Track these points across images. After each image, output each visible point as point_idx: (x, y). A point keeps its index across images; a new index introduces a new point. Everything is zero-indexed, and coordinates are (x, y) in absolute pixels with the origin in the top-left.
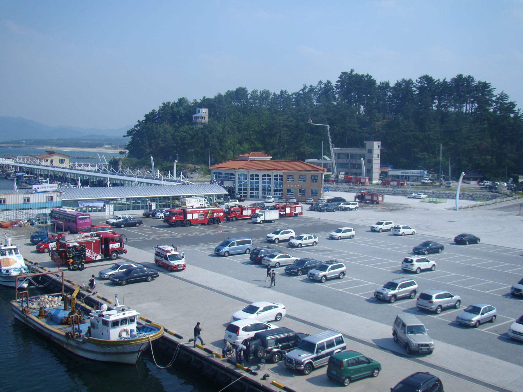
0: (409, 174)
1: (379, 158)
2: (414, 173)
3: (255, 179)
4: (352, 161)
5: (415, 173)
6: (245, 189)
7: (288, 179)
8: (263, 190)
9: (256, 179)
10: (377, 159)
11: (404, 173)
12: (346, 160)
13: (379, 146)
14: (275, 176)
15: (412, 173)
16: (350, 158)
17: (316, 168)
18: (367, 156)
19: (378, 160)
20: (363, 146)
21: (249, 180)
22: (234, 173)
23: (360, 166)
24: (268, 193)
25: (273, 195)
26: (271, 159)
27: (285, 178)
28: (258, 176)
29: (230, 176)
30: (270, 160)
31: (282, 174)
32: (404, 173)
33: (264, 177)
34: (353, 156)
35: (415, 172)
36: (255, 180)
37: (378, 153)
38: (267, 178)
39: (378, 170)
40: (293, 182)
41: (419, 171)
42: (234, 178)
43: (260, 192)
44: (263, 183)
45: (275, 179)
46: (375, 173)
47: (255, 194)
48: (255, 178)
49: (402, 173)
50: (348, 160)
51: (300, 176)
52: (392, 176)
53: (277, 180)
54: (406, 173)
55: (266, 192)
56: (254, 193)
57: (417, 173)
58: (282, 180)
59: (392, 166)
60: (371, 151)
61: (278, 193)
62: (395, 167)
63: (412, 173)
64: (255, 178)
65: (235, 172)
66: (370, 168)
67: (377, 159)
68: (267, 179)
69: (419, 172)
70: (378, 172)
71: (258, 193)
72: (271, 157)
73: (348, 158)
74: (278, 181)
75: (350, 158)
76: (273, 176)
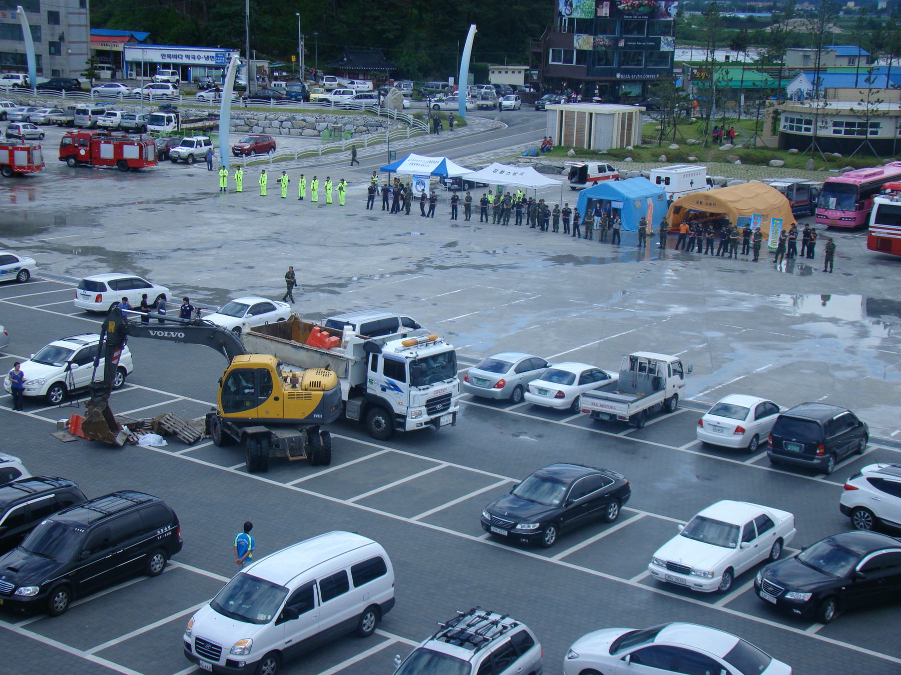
0: (185, 61)
1: (87, 10)
2: (199, 57)
10: (80, 14)
11: (169, 56)
19: (84, 16)
23: (15, 32)
32: (169, 56)
35: (202, 54)
39: (86, 44)
41: (212, 52)
46: (70, 54)
49: (163, 56)
52: (138, 64)
54: (175, 57)
57: (207, 58)
59: (142, 36)
62: (155, 40)
63: (194, 58)
66: (56, 40)
67: (80, 14)
69: (213, 54)
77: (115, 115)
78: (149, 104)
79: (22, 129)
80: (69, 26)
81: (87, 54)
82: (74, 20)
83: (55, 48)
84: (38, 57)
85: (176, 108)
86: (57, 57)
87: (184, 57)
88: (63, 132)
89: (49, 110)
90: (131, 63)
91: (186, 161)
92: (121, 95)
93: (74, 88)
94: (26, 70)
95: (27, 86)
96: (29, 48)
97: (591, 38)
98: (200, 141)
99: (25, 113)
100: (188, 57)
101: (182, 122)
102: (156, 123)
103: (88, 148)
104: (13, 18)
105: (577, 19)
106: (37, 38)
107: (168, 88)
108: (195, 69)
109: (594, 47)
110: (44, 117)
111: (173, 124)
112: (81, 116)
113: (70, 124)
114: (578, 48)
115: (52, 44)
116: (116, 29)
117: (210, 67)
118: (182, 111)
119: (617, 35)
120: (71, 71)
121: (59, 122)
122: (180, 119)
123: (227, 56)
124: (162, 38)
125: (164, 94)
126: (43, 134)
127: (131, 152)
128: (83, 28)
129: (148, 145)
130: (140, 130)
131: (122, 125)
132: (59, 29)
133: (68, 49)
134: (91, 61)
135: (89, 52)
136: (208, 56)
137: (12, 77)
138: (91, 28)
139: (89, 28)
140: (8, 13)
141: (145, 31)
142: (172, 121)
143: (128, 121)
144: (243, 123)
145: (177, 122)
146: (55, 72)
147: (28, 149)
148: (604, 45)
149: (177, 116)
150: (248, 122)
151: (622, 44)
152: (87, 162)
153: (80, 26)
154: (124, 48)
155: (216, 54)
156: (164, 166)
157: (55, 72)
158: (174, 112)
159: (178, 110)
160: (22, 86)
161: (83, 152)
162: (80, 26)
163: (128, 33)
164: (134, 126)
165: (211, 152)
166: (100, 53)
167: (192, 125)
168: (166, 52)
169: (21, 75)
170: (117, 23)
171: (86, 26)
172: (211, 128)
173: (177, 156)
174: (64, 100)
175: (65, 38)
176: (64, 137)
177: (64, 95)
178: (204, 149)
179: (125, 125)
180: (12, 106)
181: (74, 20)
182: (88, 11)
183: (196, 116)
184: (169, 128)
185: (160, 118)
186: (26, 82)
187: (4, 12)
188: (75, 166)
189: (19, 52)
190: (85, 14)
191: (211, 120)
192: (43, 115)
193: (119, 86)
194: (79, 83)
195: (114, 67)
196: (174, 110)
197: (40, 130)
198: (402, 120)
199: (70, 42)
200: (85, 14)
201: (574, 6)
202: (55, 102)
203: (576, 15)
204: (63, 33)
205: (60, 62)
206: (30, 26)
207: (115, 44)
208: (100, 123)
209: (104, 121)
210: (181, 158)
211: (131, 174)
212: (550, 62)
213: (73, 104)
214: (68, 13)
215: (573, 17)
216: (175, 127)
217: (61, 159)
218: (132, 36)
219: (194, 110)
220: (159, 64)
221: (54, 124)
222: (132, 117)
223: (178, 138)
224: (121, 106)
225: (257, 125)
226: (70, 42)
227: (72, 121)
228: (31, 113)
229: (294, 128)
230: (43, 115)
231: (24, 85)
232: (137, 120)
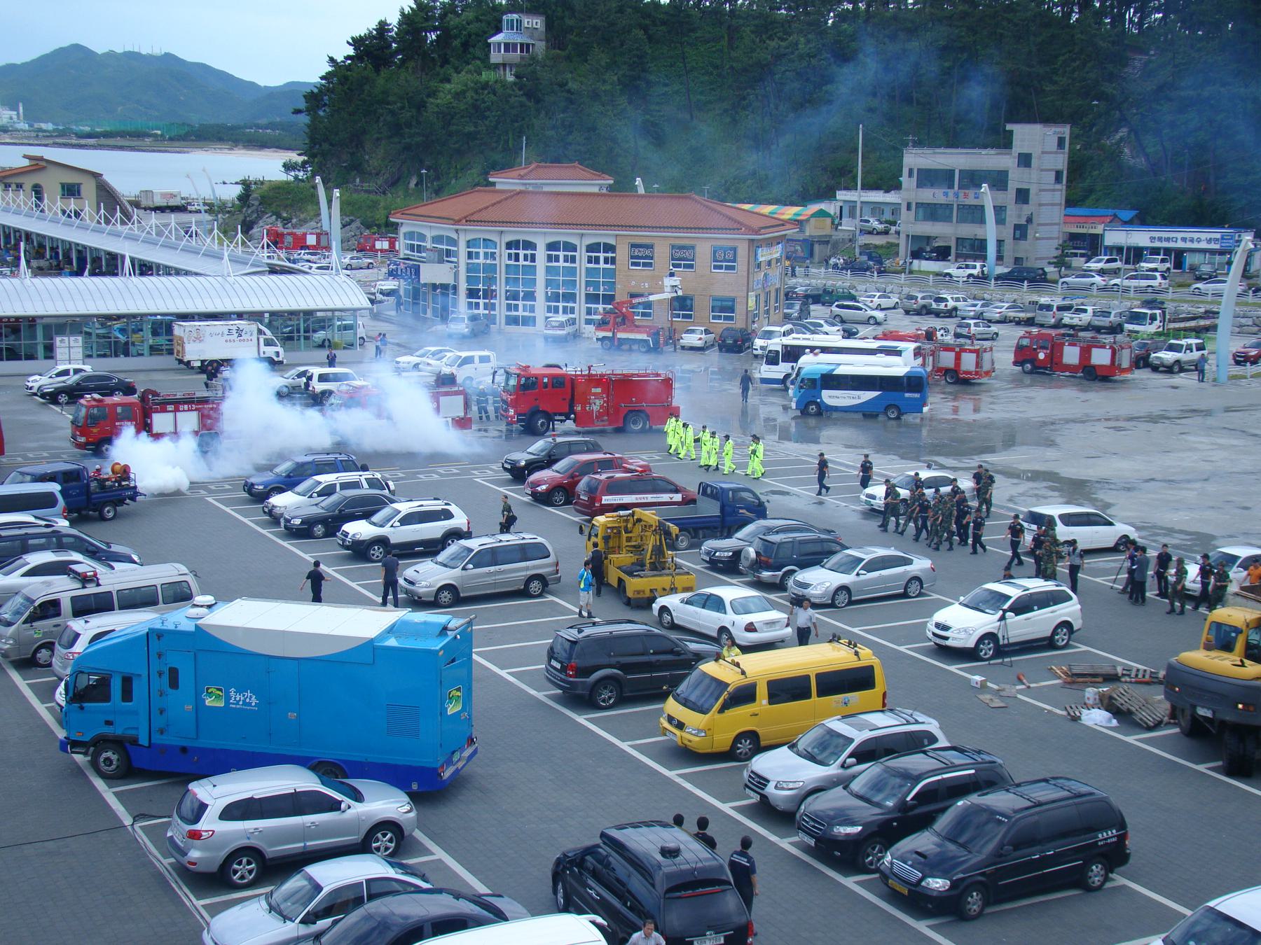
0: (1180, 245)
1: (1062, 187)
2: (1199, 240)
3: (521, 257)
4: (966, 196)
5: (1202, 238)
6: (489, 294)
7: (632, 257)
8: (548, 299)
9: (526, 259)
10: (1054, 190)
11: (1160, 239)
12: (946, 194)
13: (1061, 142)
14: (591, 248)
15: (1192, 240)
17: (730, 218)
20: (1005, 142)
21: (503, 258)
22: (454, 236)
23: (975, 214)
24: (565, 310)
25: (584, 316)
26: (610, 188)
27: (622, 254)
28: (529, 245)
29: (445, 247)
30: (604, 191)
31: (612, 241)
32: (1160, 239)
33: (554, 253)
34: (973, 179)
35: (1203, 236)
36: (522, 262)
37: (1060, 167)
38: (561, 254)
39: (1057, 227)
40: (647, 271)
41: (1216, 233)
42: (456, 254)
43: (540, 303)
44: (548, 270)
45: (590, 261)
46: (1038, 239)
47: (524, 310)
48: (522, 253)
49: (1152, 239)
50: (951, 193)
51: (673, 247)
52: (1119, 250)
53: (597, 260)
54: (1168, 240)
55: (561, 305)
56: (521, 308)
58: (613, 261)
59: (1127, 215)
60: (1025, 160)
61: (601, 307)
62: (1144, 219)
63: (1192, 240)
64: (522, 253)
65: (457, 231)
66: (1023, 222)
67: (1054, 190)
68: (561, 259)
69: (1218, 236)
70: (1055, 235)
71: (532, 309)
72: (612, 182)
73: (951, 186)
74: (602, 265)
76: (584, 249)
77: (1085, 311)
78: (1129, 299)
79: (973, 328)
80: (1040, 205)
81: (1058, 238)
83: (1021, 232)
84: (1000, 243)
85: (1163, 303)
87: (1179, 240)
88: (1021, 331)
89: (1007, 305)
90: (1110, 249)
91: (1169, 369)
92: (1095, 287)
93: (1038, 279)
94: (984, 258)
95: (983, 278)
96: (990, 232)
98: (1191, 344)
99: (977, 308)
100: (1184, 240)
101: (1169, 319)
102: (1135, 322)
103: (1048, 351)
104: (975, 198)
106: (1000, 221)
107: (1154, 278)
108: (1193, 255)
110: (1000, 313)
111: (1157, 323)
112: (1044, 312)
113: (1030, 322)
115: (1017, 227)
116: (1097, 207)
117: (1212, 252)
118: (1170, 307)
120: (1036, 259)
121: (1017, 319)
122: (1167, 317)
123: (1237, 238)
124: (1154, 218)
125: (1149, 286)
126: (997, 334)
127: (1100, 357)
128: (1057, 208)
129: (1122, 348)
130: (1115, 329)
131: (1092, 323)
132: (1027, 210)
133: (1036, 233)
134: (1063, 247)
135: (1061, 236)
136: (1210, 239)
137: (967, 267)
138: (1066, 207)
139: (1063, 207)
140: (971, 193)
141: (1133, 208)
142: (1156, 320)
143: (1101, 318)
144: (1250, 323)
145: (1163, 321)
146: (1018, 260)
147: (977, 352)
149: (1164, 313)
150: (1257, 322)
152: (1046, 368)
153: (1053, 205)
154: (1104, 230)
155: (1222, 238)
156: (1142, 375)
157: (1018, 260)
158: (1160, 309)
159: (1165, 306)
160: (977, 277)
161: (1041, 356)
162: (1053, 205)
163: (1110, 212)
164: (1107, 324)
165: (1203, 359)
166: (1073, 237)
167: (1182, 325)
168: (1157, 235)
169: (978, 264)
170: (1097, 200)
172: (1207, 329)
173: (1159, 363)
174: (1025, 294)
176: (1021, 338)
177: (1025, 287)
178: (1196, 355)
179: (1097, 323)
180: (965, 300)
181: (1046, 198)
182: (1064, 187)
183: (1189, 313)
184: (1152, 328)
185: (1142, 315)
186: (983, 272)
187: (967, 191)
188: (1030, 373)
189: (978, 237)
190: (1061, 190)
191: (1208, 318)
192: (999, 310)
193: (1093, 277)
194: (1045, 273)
195: (1089, 253)
196: (1160, 306)
197: (994, 328)
199: (1039, 225)
200: (1061, 190)
202: (1015, 296)
204: (1032, 214)
205: (1024, 248)
206: (994, 207)
207: (1093, 225)
208: (1066, 321)
209: (1072, 318)
210: (1164, 366)
211: (1099, 384)
213: (1035, 298)
214: (1040, 190)
216: (1159, 327)
217: (1015, 363)
218: (1115, 216)
219: (1186, 306)
220: (1147, 248)
221: (1011, 321)
222: (1106, 314)
223: (1164, 339)
224: (1094, 300)
226: (1039, 225)
227: (1033, 318)
228: (985, 309)
230: (999, 310)
231: (980, 275)
232: (1112, 318)
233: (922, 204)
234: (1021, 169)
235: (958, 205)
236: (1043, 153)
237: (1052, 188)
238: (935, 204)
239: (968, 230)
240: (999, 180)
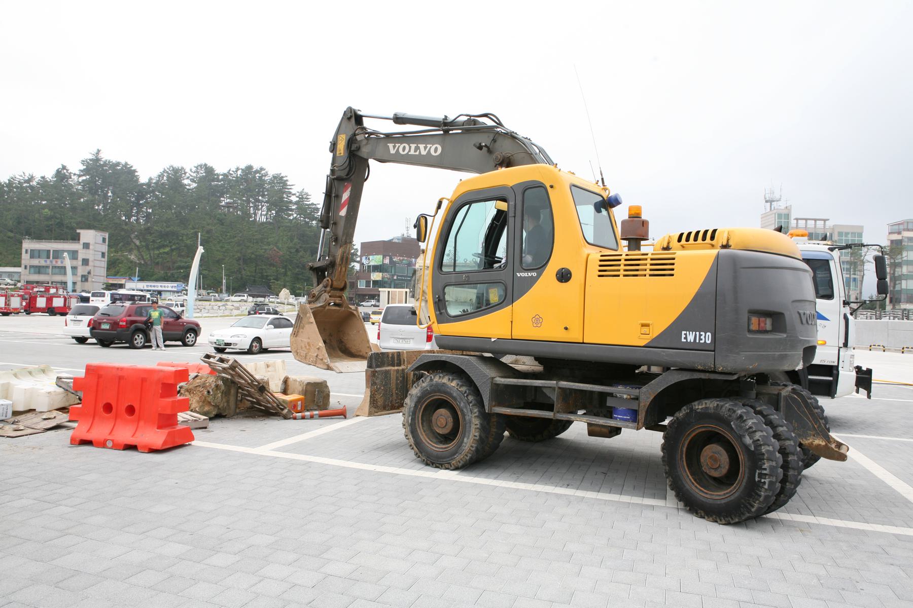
4: (56, 262)
10: (101, 261)
12: (46, 261)
13: (104, 240)
16: (51, 258)
18: (82, 254)
20: (76, 238)
37: (104, 251)
46: (93, 282)
50: (48, 261)
67: (101, 261)
75: (51, 258)
80: (94, 266)
82: (97, 264)
83: (85, 278)
84: (74, 283)
86: (86, 283)
97: (381, 274)
105: (373, 266)
106: (74, 274)
109: (382, 278)
114: (373, 279)
115: (83, 276)
119: (393, 273)
132: (88, 268)
148: (387, 278)
150: (199, 307)
151: (395, 278)
153: (101, 267)
162: (101, 267)
171: (104, 268)
175: (92, 273)
181: (97, 264)
190: (104, 261)
198: (290, 305)
199: (94, 275)
200: (104, 261)
201: (371, 259)
203: (372, 264)
212: (359, 287)
215: (370, 264)
225: (205, 308)
226: (94, 275)
229: (226, 310)
233: (33, 266)
234: (85, 251)
235: (52, 267)
236: (96, 243)
237: (99, 259)
238: (40, 266)
239: (58, 278)
240: (74, 255)
